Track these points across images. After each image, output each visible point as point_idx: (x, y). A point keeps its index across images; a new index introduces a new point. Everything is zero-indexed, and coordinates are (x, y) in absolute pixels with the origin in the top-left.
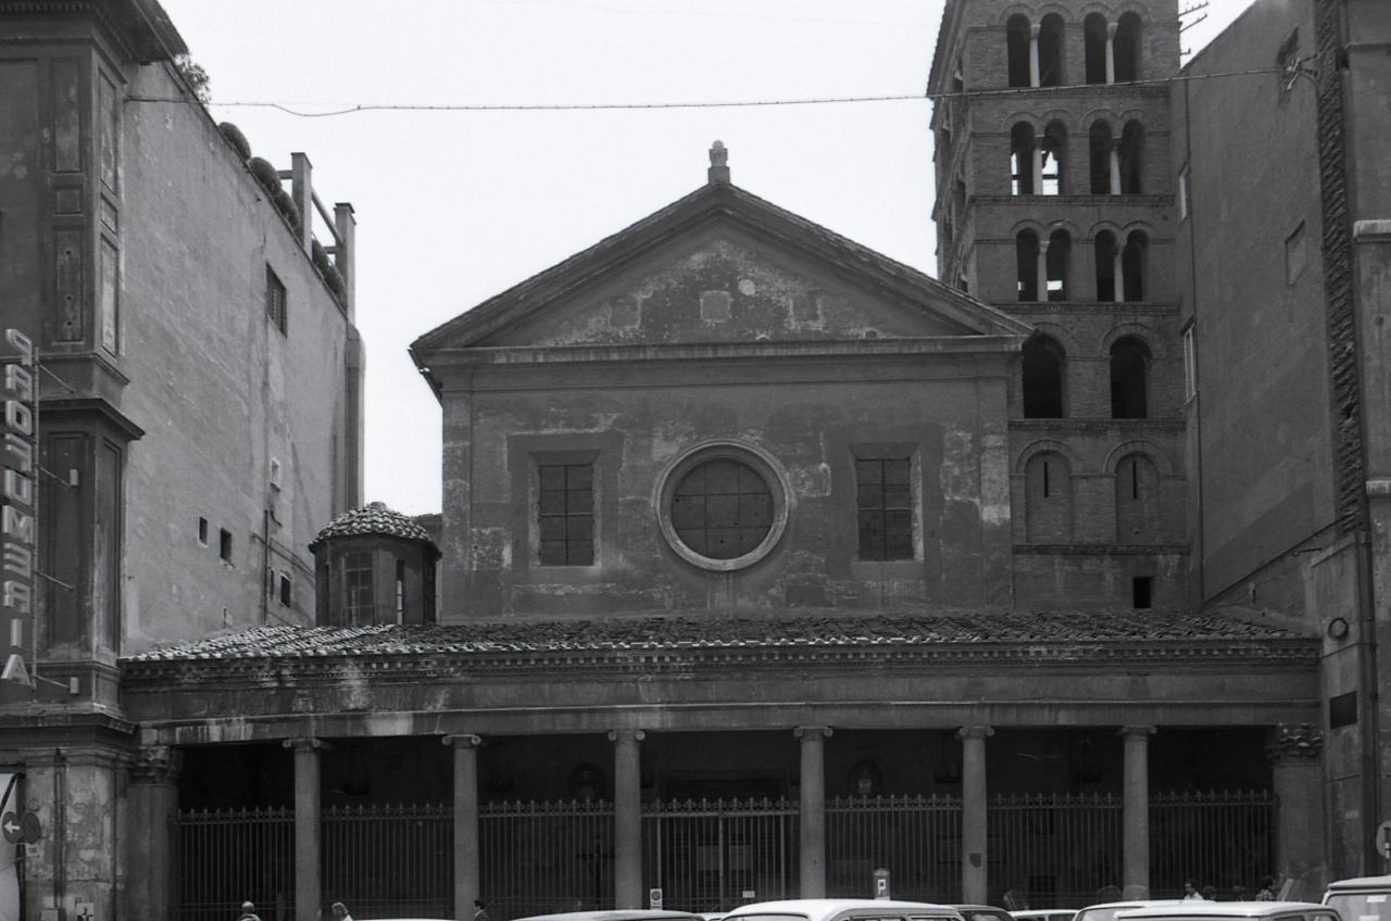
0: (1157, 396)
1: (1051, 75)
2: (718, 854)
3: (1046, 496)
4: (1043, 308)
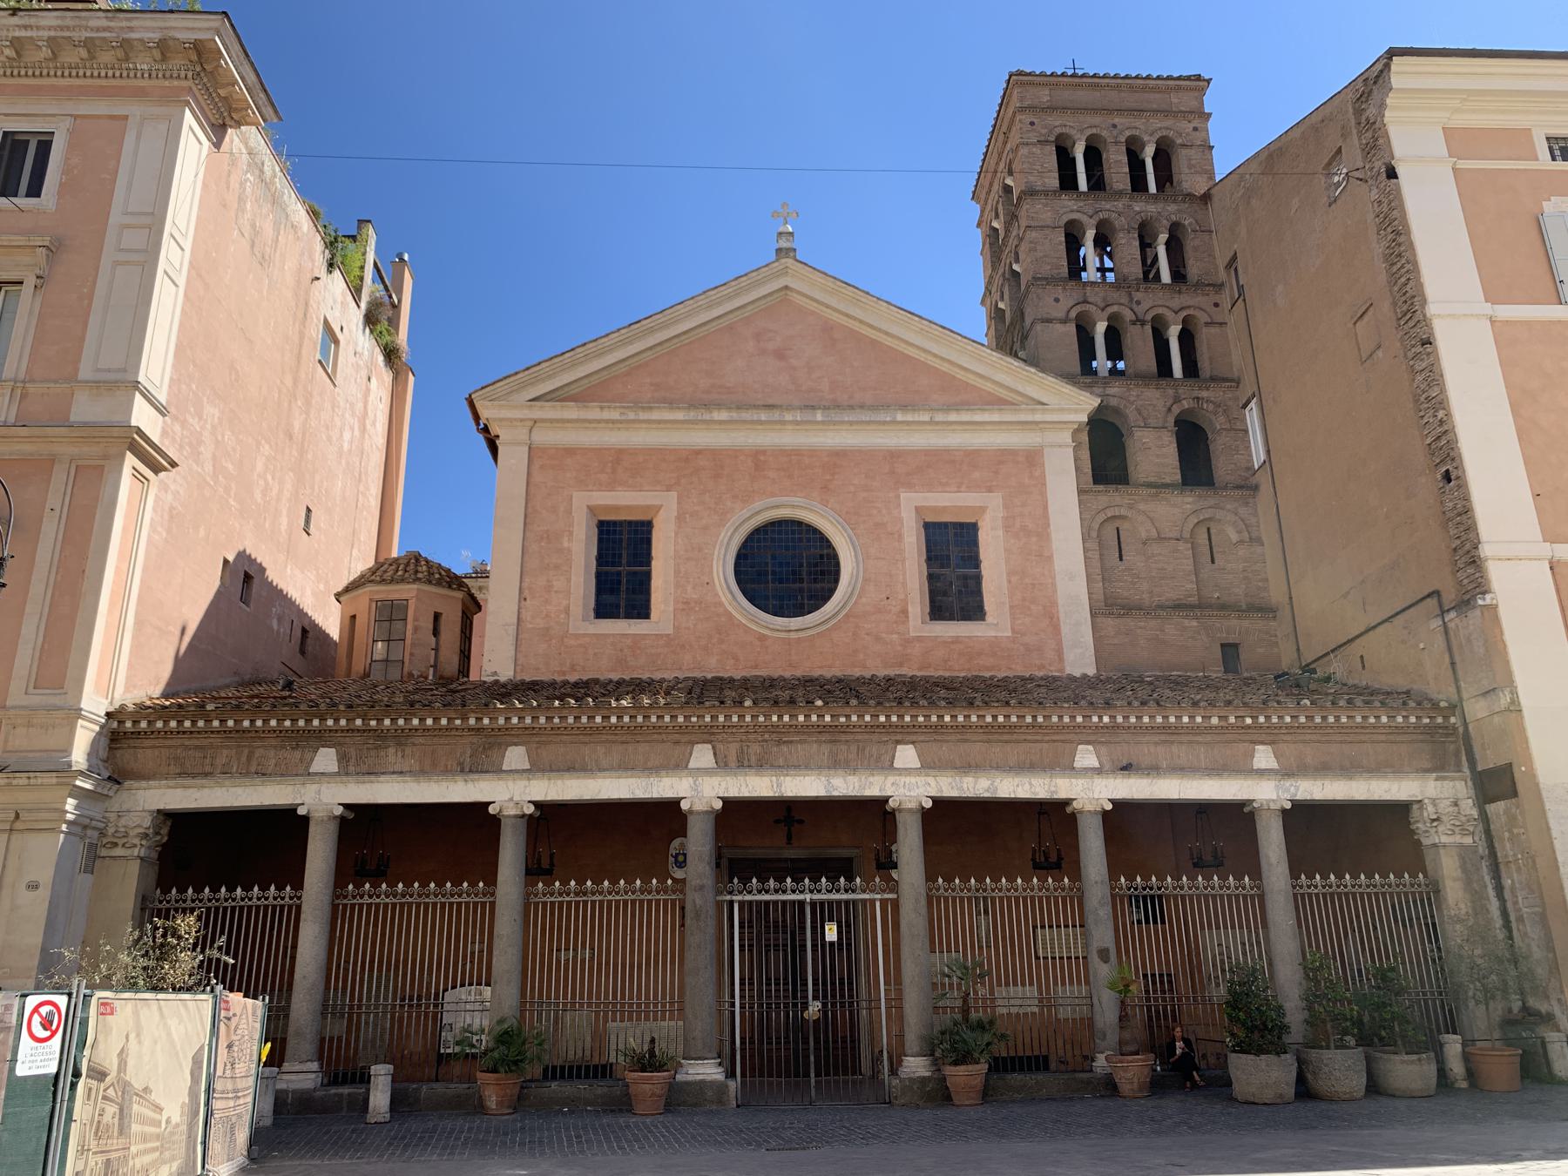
0: (1222, 467)
1: (1097, 183)
2: (805, 946)
3: (1121, 559)
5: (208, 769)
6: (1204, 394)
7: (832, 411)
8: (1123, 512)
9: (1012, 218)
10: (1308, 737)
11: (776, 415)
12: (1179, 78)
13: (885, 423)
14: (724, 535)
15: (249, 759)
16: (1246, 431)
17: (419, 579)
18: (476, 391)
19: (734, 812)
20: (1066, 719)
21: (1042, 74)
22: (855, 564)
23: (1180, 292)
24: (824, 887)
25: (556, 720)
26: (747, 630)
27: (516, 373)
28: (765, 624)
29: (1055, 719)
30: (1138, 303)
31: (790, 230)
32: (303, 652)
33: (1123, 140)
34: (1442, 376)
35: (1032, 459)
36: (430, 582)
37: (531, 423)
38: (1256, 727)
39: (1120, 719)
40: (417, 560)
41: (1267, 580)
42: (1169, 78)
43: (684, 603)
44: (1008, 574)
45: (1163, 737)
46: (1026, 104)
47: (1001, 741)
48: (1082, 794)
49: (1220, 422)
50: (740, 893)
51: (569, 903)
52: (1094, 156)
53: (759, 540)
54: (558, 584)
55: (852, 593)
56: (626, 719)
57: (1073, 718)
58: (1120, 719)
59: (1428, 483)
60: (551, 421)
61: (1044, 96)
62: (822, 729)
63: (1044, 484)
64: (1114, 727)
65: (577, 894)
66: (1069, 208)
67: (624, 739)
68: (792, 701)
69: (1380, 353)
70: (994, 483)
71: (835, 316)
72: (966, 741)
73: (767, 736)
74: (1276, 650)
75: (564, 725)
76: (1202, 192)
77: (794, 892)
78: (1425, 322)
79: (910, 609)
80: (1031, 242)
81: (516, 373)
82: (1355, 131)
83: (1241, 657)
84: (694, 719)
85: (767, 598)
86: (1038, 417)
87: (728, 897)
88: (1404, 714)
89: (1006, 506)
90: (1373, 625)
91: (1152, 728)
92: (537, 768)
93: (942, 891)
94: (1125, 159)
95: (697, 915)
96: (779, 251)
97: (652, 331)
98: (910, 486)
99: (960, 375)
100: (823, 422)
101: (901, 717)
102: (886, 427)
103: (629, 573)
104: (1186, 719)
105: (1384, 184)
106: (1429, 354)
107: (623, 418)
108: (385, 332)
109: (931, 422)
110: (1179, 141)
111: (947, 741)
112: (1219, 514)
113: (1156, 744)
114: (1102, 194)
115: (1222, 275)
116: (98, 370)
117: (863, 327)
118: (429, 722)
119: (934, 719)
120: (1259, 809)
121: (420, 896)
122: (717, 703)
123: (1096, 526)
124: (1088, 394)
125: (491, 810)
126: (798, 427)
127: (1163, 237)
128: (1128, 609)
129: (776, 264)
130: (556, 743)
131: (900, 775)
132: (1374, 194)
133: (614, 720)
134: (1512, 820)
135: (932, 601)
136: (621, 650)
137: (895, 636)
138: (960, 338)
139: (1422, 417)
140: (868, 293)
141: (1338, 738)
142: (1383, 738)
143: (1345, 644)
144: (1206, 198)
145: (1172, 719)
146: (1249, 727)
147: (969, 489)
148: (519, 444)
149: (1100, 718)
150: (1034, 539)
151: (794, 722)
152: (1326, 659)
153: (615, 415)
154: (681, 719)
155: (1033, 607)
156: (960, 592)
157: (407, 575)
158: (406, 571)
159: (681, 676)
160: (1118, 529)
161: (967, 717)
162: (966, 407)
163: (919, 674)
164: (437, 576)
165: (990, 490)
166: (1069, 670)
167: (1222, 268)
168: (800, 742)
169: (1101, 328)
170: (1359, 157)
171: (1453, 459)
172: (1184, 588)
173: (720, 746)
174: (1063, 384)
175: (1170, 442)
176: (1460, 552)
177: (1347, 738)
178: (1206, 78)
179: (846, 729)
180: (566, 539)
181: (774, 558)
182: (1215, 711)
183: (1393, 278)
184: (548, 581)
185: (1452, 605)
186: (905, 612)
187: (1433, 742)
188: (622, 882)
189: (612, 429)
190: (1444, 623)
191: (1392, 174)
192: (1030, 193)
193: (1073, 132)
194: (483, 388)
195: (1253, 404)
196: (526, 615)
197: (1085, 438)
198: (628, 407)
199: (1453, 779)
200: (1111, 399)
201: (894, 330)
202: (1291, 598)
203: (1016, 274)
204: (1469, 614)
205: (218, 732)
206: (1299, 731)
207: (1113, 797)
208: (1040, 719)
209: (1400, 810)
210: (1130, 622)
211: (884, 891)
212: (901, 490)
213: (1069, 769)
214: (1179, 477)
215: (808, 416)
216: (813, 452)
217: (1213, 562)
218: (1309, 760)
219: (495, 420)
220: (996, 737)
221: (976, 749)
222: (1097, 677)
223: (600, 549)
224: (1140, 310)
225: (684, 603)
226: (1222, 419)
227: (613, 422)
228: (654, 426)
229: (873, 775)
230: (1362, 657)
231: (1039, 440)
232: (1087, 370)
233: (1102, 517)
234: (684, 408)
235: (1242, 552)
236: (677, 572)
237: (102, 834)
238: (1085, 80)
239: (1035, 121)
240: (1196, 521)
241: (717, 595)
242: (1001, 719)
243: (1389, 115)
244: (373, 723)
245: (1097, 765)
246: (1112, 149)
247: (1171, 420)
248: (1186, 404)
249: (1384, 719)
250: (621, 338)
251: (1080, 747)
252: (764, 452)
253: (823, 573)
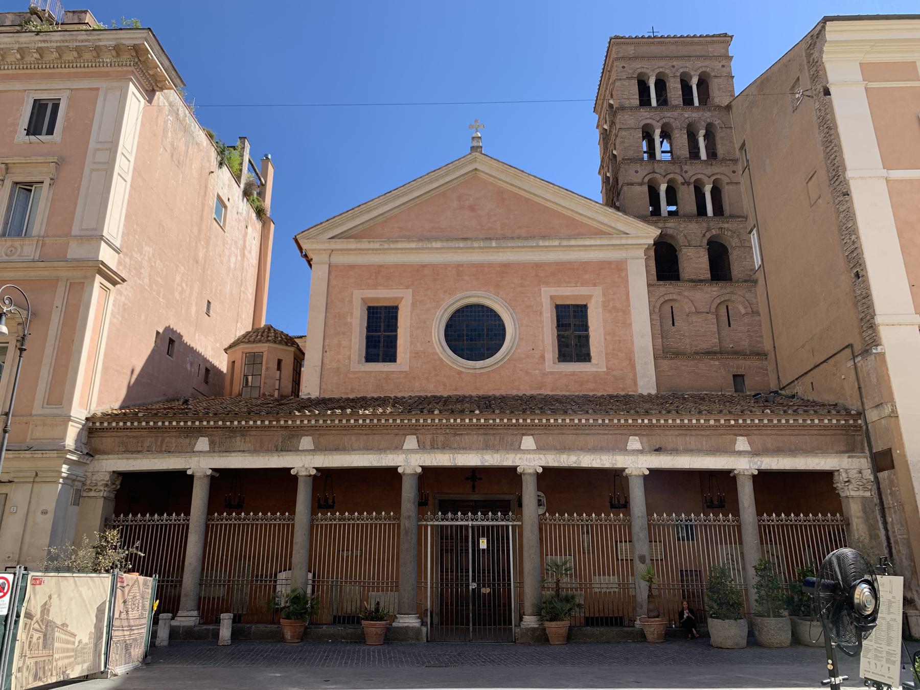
0: (736, 269)
1: (663, 100)
2: (468, 550)
3: (673, 324)
4: (665, 220)
5: (140, 449)
6: (726, 225)
7: (501, 241)
8: (675, 297)
9: (613, 123)
10: (769, 432)
11: (469, 244)
12: (713, 36)
13: (532, 247)
14: (439, 313)
15: (162, 443)
16: (751, 247)
17: (270, 340)
18: (299, 234)
19: (429, 474)
20: (622, 421)
21: (630, 38)
22: (514, 330)
23: (711, 165)
24: (479, 517)
25: (329, 422)
26: (451, 368)
27: (321, 223)
28: (461, 365)
29: (616, 421)
30: (686, 172)
31: (480, 136)
32: (206, 382)
33: (678, 74)
34: (855, 214)
35: (619, 267)
36: (275, 342)
37: (330, 252)
38: (737, 426)
39: (654, 421)
40: (269, 329)
41: (762, 336)
42: (707, 36)
43: (415, 353)
44: (605, 335)
45: (681, 432)
46: (620, 55)
47: (582, 434)
48: (631, 465)
49: (735, 242)
50: (432, 520)
51: (335, 525)
52: (661, 84)
53: (459, 317)
54: (345, 343)
55: (512, 347)
56: (368, 421)
57: (626, 420)
58: (654, 421)
59: (846, 279)
60: (341, 250)
61: (631, 50)
62: (479, 427)
63: (627, 281)
64: (651, 426)
65: (340, 520)
66: (646, 116)
67: (367, 432)
68: (462, 411)
69: (820, 201)
70: (597, 281)
71: (505, 185)
72: (563, 434)
73: (448, 431)
74: (766, 379)
75: (333, 424)
76: (726, 104)
77: (462, 520)
78: (845, 182)
79: (546, 355)
80: (621, 138)
81: (321, 223)
82: (806, 67)
83: (746, 383)
84: (406, 421)
85: (463, 350)
86: (624, 242)
87: (425, 523)
88: (829, 418)
89: (604, 294)
90: (817, 364)
91: (674, 427)
92: (319, 449)
93: (548, 520)
94: (679, 86)
95: (407, 533)
96: (472, 148)
97: (398, 197)
98: (547, 284)
99: (578, 217)
100: (496, 247)
101: (525, 420)
102: (534, 250)
103: (385, 336)
104: (694, 421)
105: (822, 99)
106: (847, 201)
107: (381, 247)
108: (256, 200)
109: (560, 246)
110: (713, 74)
111: (552, 434)
112: (734, 297)
113: (677, 436)
114: (665, 108)
116: (82, 230)
117: (521, 191)
118: (259, 423)
119: (544, 421)
120: (739, 474)
121: (253, 520)
122: (419, 412)
123: (658, 305)
124: (653, 228)
125: (292, 472)
126: (482, 250)
127: (702, 132)
128: (677, 354)
129: (470, 156)
130: (329, 435)
131: (524, 453)
132: (817, 105)
133: (361, 422)
134: (892, 483)
135: (560, 351)
136: (380, 380)
137: (537, 371)
138: (577, 196)
139: (843, 239)
140: (523, 171)
141: (788, 432)
142: (815, 432)
143: (803, 375)
144: (728, 108)
145: (686, 421)
146: (733, 426)
147: (583, 285)
148: (323, 263)
149: (643, 420)
150: (621, 314)
151: (463, 423)
152: (793, 384)
153: (377, 246)
154: (398, 421)
155: (619, 354)
156: (576, 345)
157: (263, 338)
158: (262, 336)
159: (413, 395)
160: (672, 307)
161: (563, 420)
162: (581, 237)
163: (551, 393)
164: (280, 339)
165: (595, 285)
166: (640, 391)
167: (737, 150)
168: (467, 434)
169: (663, 188)
170: (809, 83)
171: (860, 265)
172: (711, 342)
173: (421, 437)
174: (638, 222)
175: (704, 255)
176: (865, 321)
177: (793, 433)
178: (730, 35)
179: (493, 427)
180: (349, 317)
181: (467, 326)
182: (712, 417)
183: (828, 156)
184: (339, 341)
185: (860, 352)
187: (847, 435)
188: (365, 513)
189: (376, 254)
190: (855, 363)
191: (827, 92)
192: (622, 108)
193: (648, 71)
194: (302, 232)
195: (755, 232)
196: (327, 361)
197: (652, 253)
198: (384, 241)
199: (859, 458)
200: (669, 229)
201: (538, 192)
202: (775, 347)
203: (615, 156)
204: (868, 358)
205: (145, 428)
206: (763, 428)
207: (650, 467)
208: (607, 421)
209: (827, 476)
210: (678, 363)
211: (514, 520)
212: (542, 286)
213: (624, 450)
214: (709, 275)
215: (487, 244)
216: (491, 265)
217: (730, 326)
218: (770, 445)
219: (310, 250)
220: (581, 432)
221: (569, 439)
222: (657, 396)
223: (368, 322)
224: (687, 176)
225: (415, 353)
226: (736, 240)
227: (376, 250)
228: (399, 252)
229: (508, 454)
230: (812, 383)
231: (624, 255)
233: (662, 300)
234: (416, 241)
235: (747, 319)
236: (411, 335)
237: (84, 484)
238: (656, 40)
239: (625, 65)
240: (719, 302)
241: (434, 348)
242: (583, 421)
243: (825, 57)
244: (228, 423)
245: (641, 448)
246: (672, 80)
247: (705, 241)
248: (714, 232)
249: (816, 421)
250: (380, 202)
251: (631, 437)
252: (462, 266)
253: (495, 335)
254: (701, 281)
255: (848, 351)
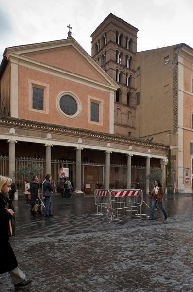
19: (85, 151)
35: (108, 95)
54: (26, 99)
61: (115, 21)
64: (135, 144)
98: (90, 95)
115: (136, 69)
169: (119, 73)
186: (88, 119)
232: (116, 81)
254: (125, 105)
255: (169, 132)
